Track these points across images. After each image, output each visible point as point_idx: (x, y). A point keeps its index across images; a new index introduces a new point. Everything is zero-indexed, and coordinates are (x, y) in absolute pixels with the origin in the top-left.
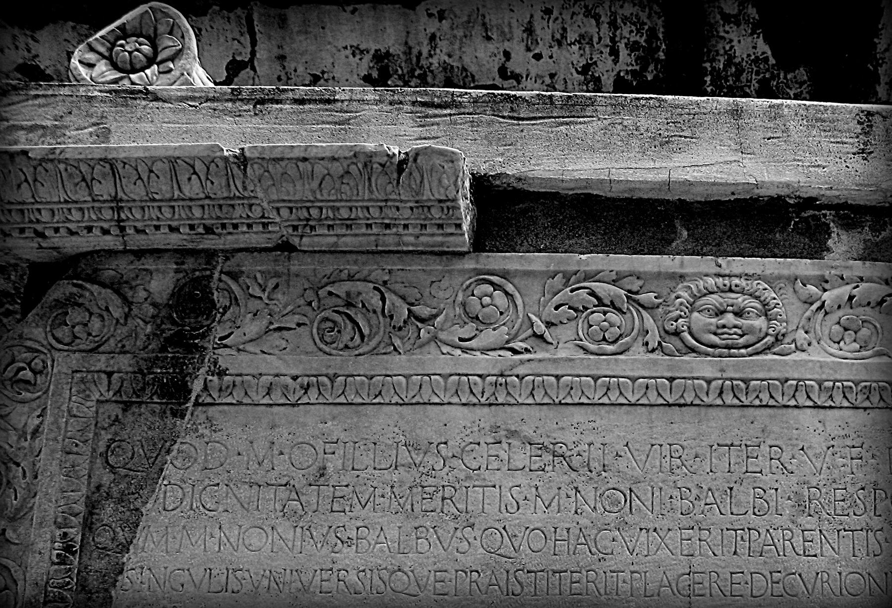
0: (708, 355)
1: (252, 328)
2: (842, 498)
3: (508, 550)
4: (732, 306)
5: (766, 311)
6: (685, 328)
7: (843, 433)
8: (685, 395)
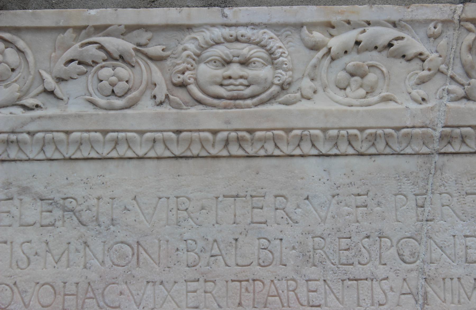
0: (214, 106)
2: (347, 247)
4: (238, 57)
6: (192, 80)
8: (191, 148)
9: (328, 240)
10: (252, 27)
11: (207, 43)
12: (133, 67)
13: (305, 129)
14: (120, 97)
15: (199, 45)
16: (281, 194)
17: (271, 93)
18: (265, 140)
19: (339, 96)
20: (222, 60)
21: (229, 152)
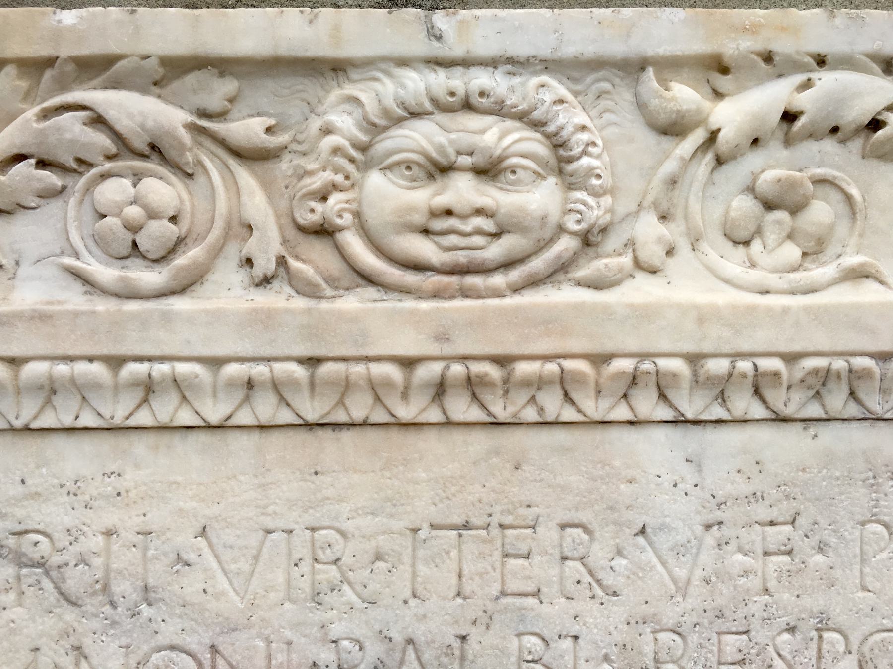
0: (406, 291)
2: (739, 657)
4: (471, 154)
6: (348, 219)
7: (745, 488)
8: (347, 402)
9: (694, 639)
10: (509, 67)
11: (386, 113)
12: (190, 176)
13: (643, 356)
14: (156, 261)
15: (365, 118)
16: (577, 522)
17: (558, 257)
18: (539, 383)
20: (428, 164)
21: (445, 413)
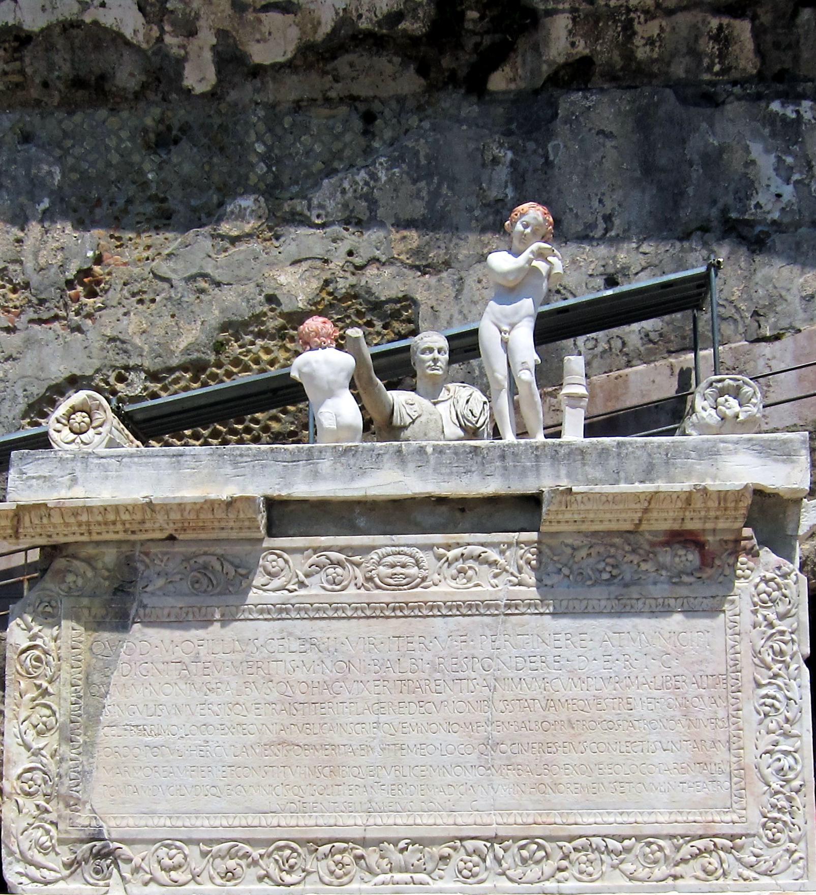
0: (387, 590)
1: (160, 582)
3: (291, 693)
5: (418, 564)
7: (456, 628)
19: (453, 583)
